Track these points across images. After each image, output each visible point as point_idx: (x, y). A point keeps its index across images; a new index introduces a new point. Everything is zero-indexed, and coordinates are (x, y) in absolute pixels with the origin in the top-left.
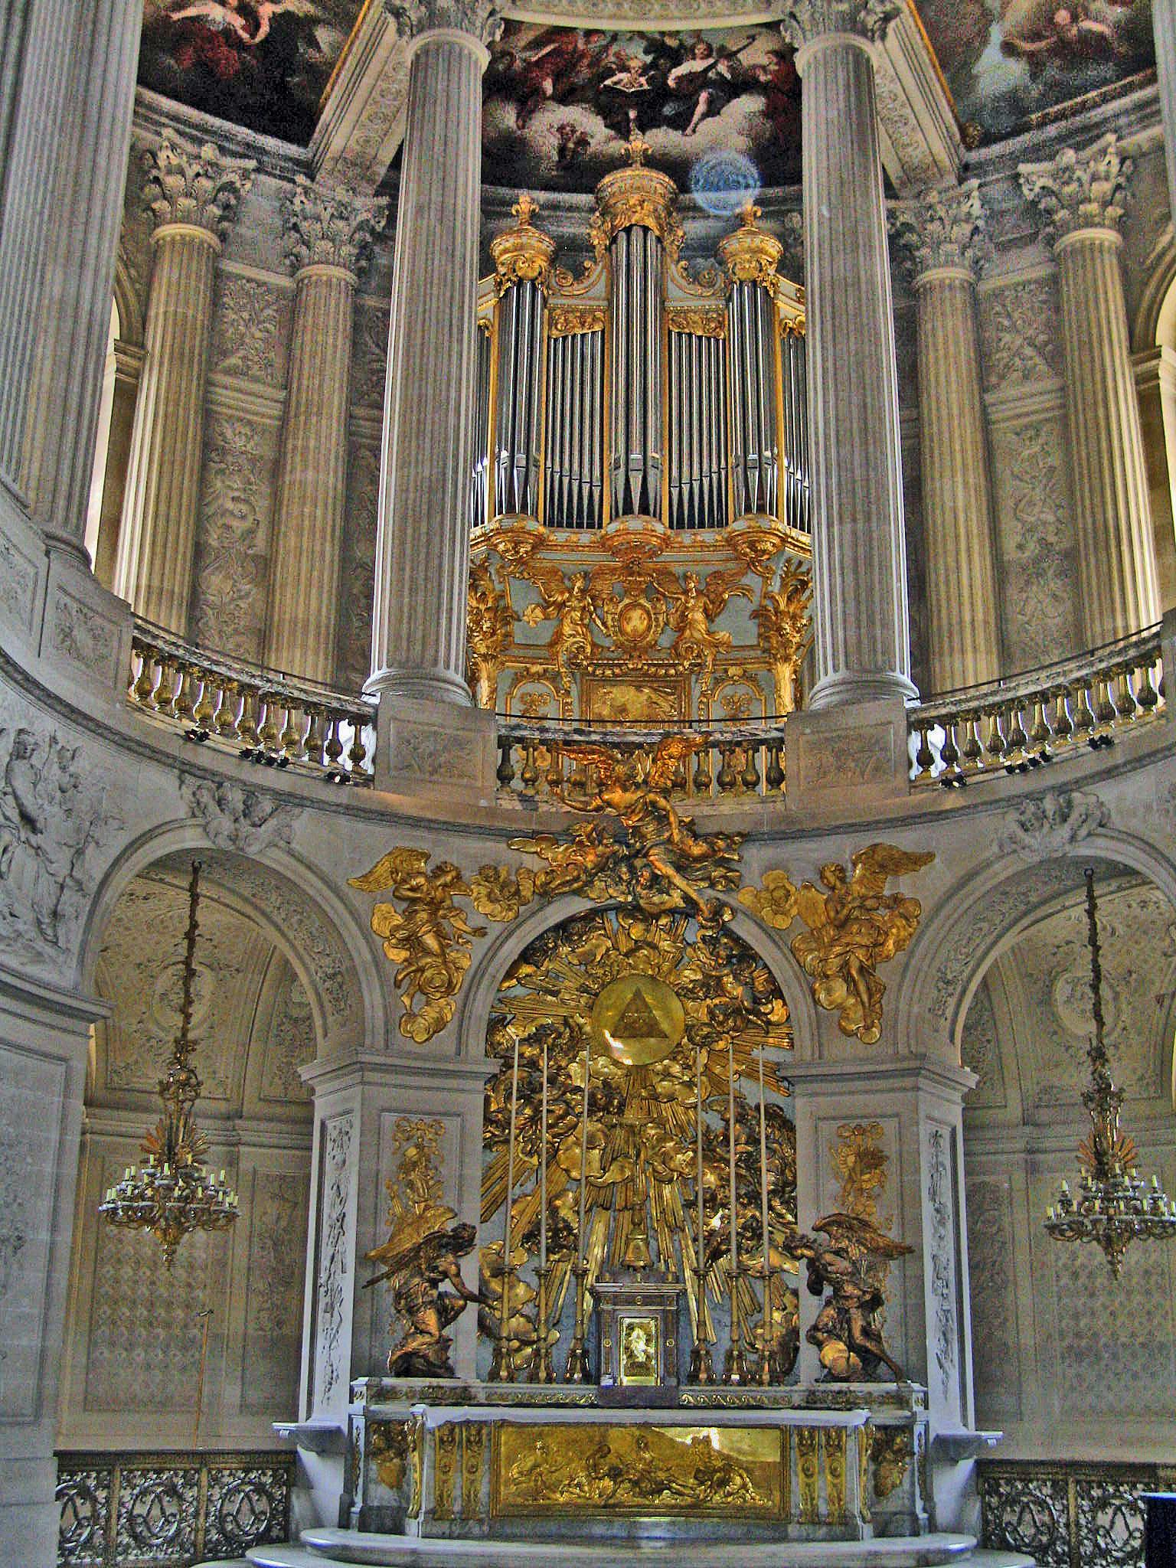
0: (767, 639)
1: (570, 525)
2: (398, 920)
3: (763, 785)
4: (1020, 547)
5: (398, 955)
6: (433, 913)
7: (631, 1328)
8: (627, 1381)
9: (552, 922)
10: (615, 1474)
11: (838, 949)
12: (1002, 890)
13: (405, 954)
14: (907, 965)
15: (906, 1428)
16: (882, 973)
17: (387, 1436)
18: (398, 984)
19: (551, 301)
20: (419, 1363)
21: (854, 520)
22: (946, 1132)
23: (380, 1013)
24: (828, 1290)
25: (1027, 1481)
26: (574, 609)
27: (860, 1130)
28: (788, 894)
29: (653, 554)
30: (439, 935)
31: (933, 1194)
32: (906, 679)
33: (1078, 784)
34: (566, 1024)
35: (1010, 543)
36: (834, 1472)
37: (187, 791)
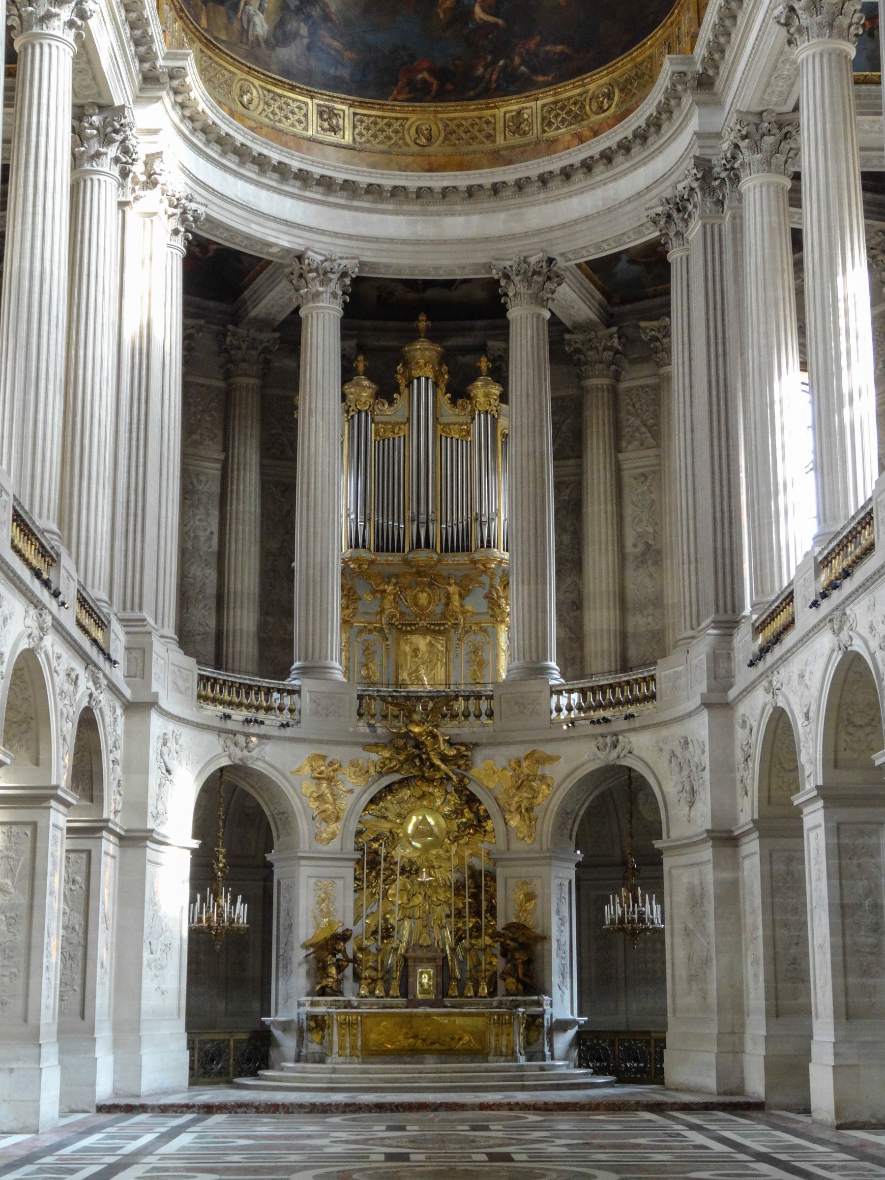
0: (492, 609)
1: (387, 551)
2: (314, 788)
3: (484, 718)
4: (635, 545)
5: (313, 805)
6: (329, 784)
7: (422, 973)
8: (420, 996)
9: (384, 785)
10: (415, 1037)
11: (516, 799)
12: (592, 774)
13: (317, 804)
14: (547, 808)
15: (541, 1015)
16: (537, 811)
17: (316, 1022)
18: (313, 819)
19: (377, 418)
20: (328, 990)
21: (529, 584)
22: (566, 883)
23: (307, 833)
24: (509, 957)
25: (598, 1040)
26: (390, 594)
27: (527, 884)
28: (494, 772)
29: (432, 567)
30: (333, 795)
31: (558, 912)
32: (553, 664)
33: (622, 732)
34: (391, 832)
35: (629, 542)
36: (508, 1035)
37: (222, 740)
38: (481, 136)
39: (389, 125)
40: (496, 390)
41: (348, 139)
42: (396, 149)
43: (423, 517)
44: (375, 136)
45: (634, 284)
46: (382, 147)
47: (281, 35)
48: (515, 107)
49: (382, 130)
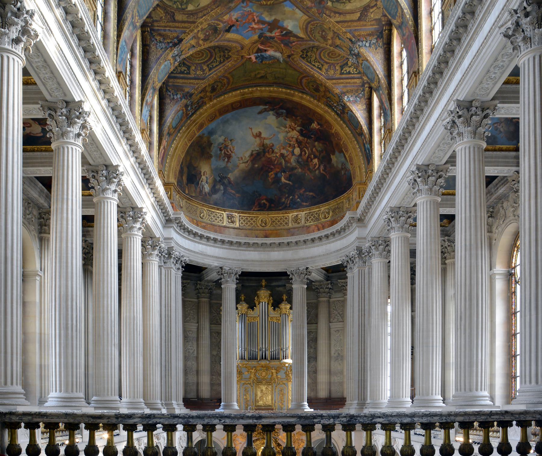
38: (284, 223)
39: (252, 219)
40: (288, 306)
41: (237, 225)
42: (254, 228)
43: (264, 350)
44: (247, 223)
45: (336, 273)
46: (249, 227)
47: (214, 190)
48: (296, 214)
49: (249, 221)
